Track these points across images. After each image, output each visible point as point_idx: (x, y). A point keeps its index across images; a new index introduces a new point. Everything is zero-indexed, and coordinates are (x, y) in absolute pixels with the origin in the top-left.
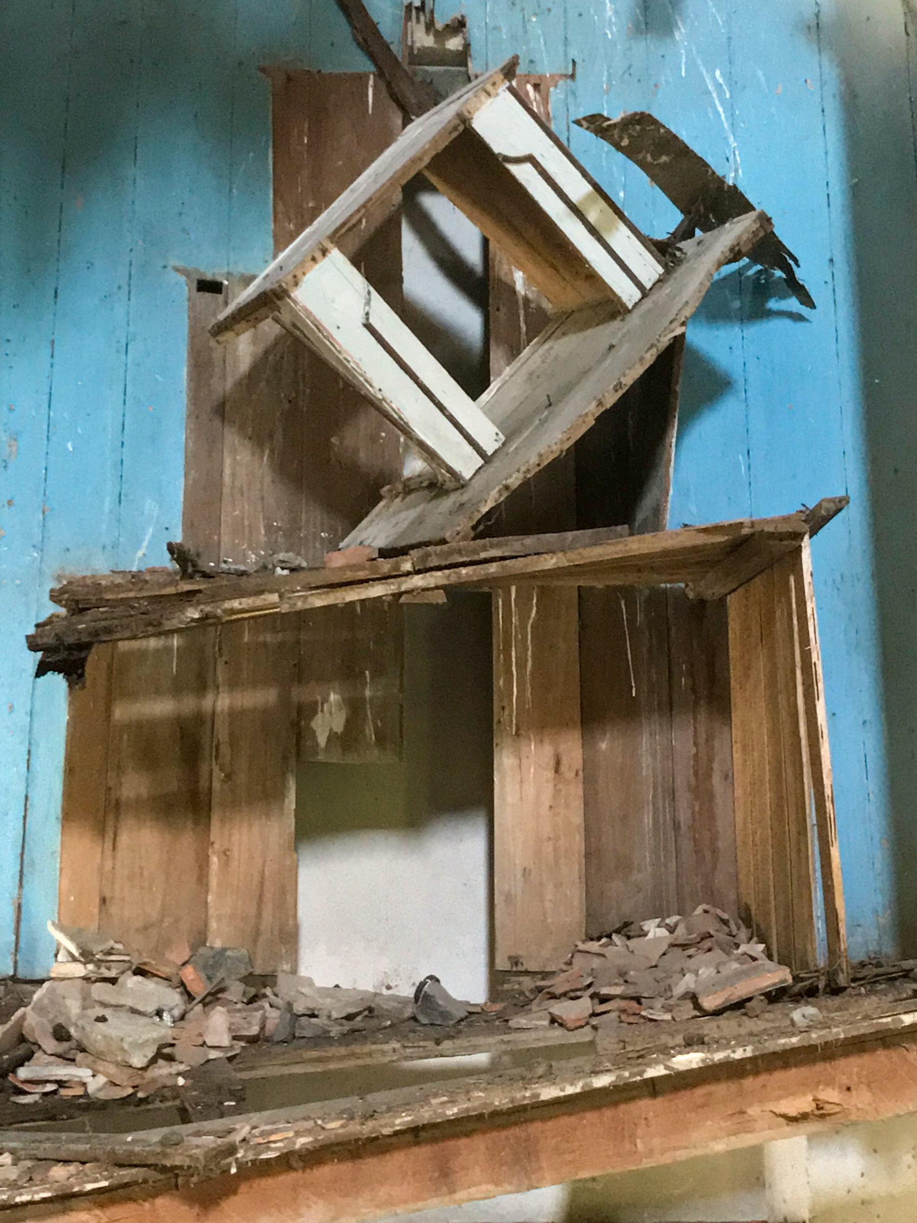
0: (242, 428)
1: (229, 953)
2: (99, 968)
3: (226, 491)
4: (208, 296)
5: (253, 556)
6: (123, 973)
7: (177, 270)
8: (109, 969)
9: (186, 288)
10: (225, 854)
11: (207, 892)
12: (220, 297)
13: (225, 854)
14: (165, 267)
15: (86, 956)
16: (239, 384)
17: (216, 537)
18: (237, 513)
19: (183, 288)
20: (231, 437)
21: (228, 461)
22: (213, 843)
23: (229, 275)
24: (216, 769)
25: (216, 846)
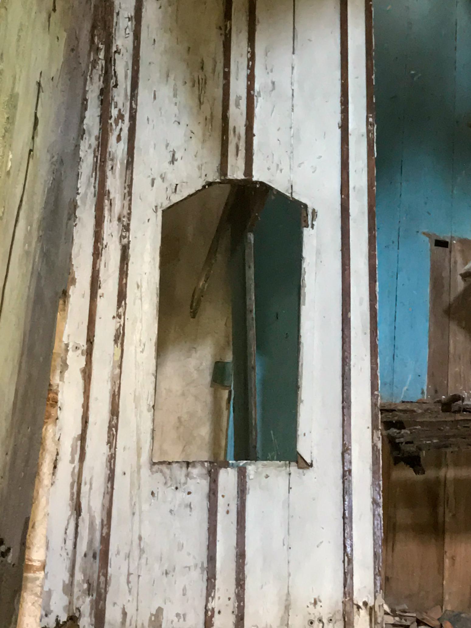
0: (459, 324)
1: (463, 615)
2: (401, 619)
3: (451, 356)
4: (441, 249)
5: (466, 394)
6: (412, 623)
7: (424, 233)
8: (406, 620)
9: (429, 244)
10: (453, 558)
11: (443, 580)
12: (447, 250)
13: (453, 558)
14: (418, 232)
15: (393, 613)
16: (457, 298)
17: (446, 382)
18: (457, 369)
19: (426, 244)
20: (453, 327)
21: (451, 342)
22: (446, 552)
23: (452, 238)
24: (447, 511)
25: (448, 554)
